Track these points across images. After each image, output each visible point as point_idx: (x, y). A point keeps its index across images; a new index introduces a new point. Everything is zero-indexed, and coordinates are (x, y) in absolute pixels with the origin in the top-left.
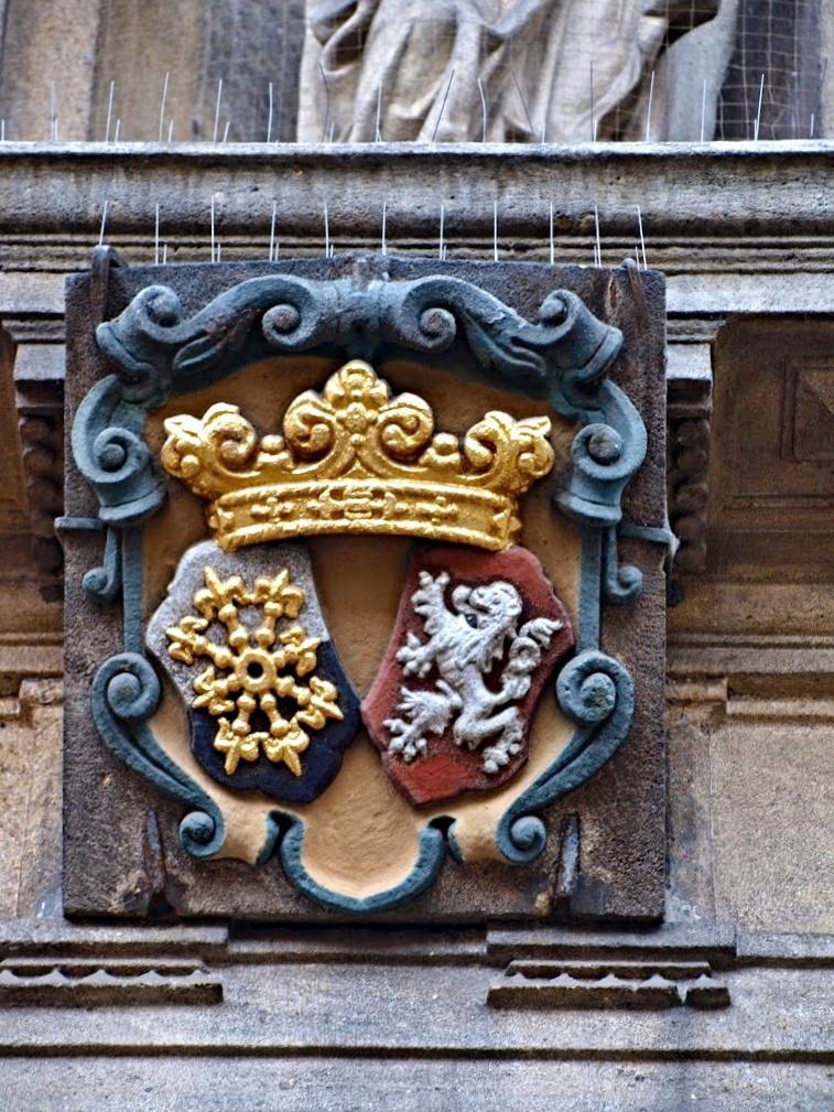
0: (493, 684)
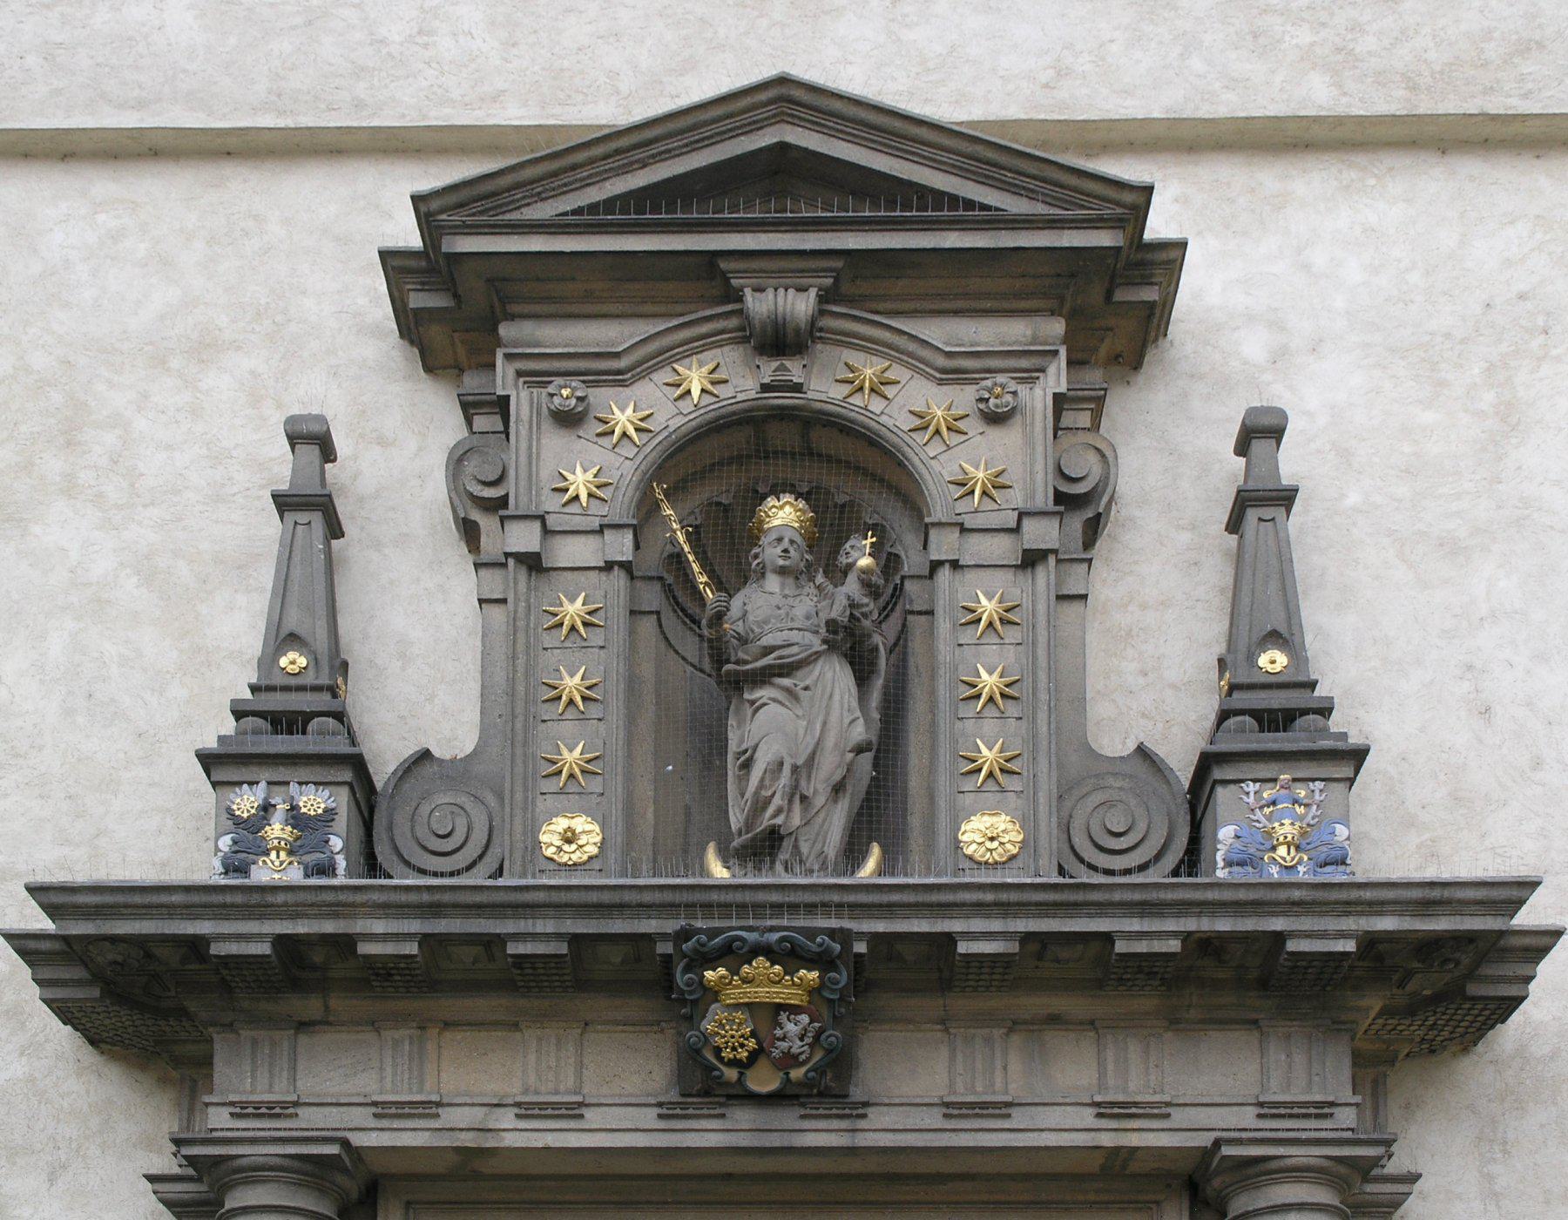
0: (801, 1039)
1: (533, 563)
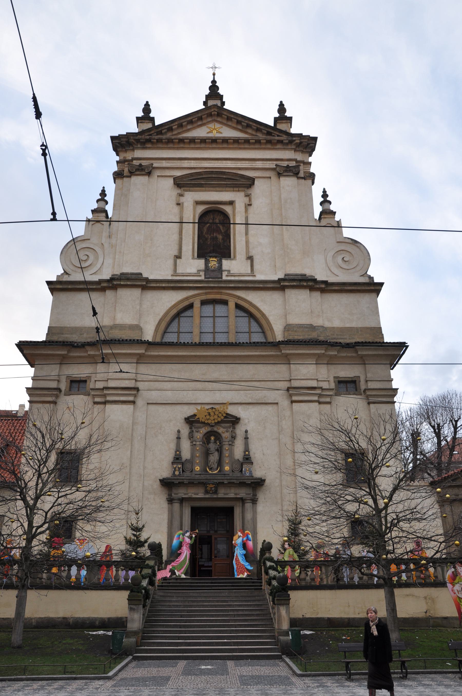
1: (195, 445)
